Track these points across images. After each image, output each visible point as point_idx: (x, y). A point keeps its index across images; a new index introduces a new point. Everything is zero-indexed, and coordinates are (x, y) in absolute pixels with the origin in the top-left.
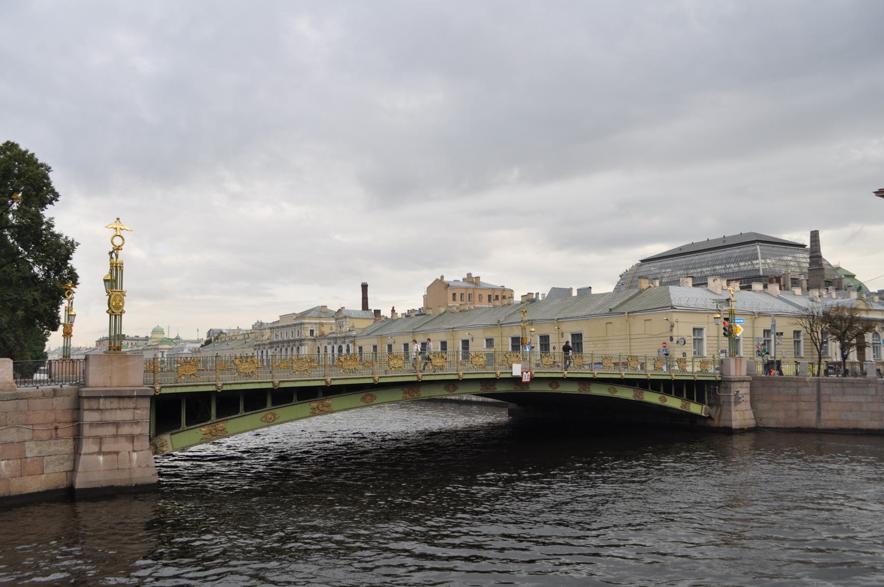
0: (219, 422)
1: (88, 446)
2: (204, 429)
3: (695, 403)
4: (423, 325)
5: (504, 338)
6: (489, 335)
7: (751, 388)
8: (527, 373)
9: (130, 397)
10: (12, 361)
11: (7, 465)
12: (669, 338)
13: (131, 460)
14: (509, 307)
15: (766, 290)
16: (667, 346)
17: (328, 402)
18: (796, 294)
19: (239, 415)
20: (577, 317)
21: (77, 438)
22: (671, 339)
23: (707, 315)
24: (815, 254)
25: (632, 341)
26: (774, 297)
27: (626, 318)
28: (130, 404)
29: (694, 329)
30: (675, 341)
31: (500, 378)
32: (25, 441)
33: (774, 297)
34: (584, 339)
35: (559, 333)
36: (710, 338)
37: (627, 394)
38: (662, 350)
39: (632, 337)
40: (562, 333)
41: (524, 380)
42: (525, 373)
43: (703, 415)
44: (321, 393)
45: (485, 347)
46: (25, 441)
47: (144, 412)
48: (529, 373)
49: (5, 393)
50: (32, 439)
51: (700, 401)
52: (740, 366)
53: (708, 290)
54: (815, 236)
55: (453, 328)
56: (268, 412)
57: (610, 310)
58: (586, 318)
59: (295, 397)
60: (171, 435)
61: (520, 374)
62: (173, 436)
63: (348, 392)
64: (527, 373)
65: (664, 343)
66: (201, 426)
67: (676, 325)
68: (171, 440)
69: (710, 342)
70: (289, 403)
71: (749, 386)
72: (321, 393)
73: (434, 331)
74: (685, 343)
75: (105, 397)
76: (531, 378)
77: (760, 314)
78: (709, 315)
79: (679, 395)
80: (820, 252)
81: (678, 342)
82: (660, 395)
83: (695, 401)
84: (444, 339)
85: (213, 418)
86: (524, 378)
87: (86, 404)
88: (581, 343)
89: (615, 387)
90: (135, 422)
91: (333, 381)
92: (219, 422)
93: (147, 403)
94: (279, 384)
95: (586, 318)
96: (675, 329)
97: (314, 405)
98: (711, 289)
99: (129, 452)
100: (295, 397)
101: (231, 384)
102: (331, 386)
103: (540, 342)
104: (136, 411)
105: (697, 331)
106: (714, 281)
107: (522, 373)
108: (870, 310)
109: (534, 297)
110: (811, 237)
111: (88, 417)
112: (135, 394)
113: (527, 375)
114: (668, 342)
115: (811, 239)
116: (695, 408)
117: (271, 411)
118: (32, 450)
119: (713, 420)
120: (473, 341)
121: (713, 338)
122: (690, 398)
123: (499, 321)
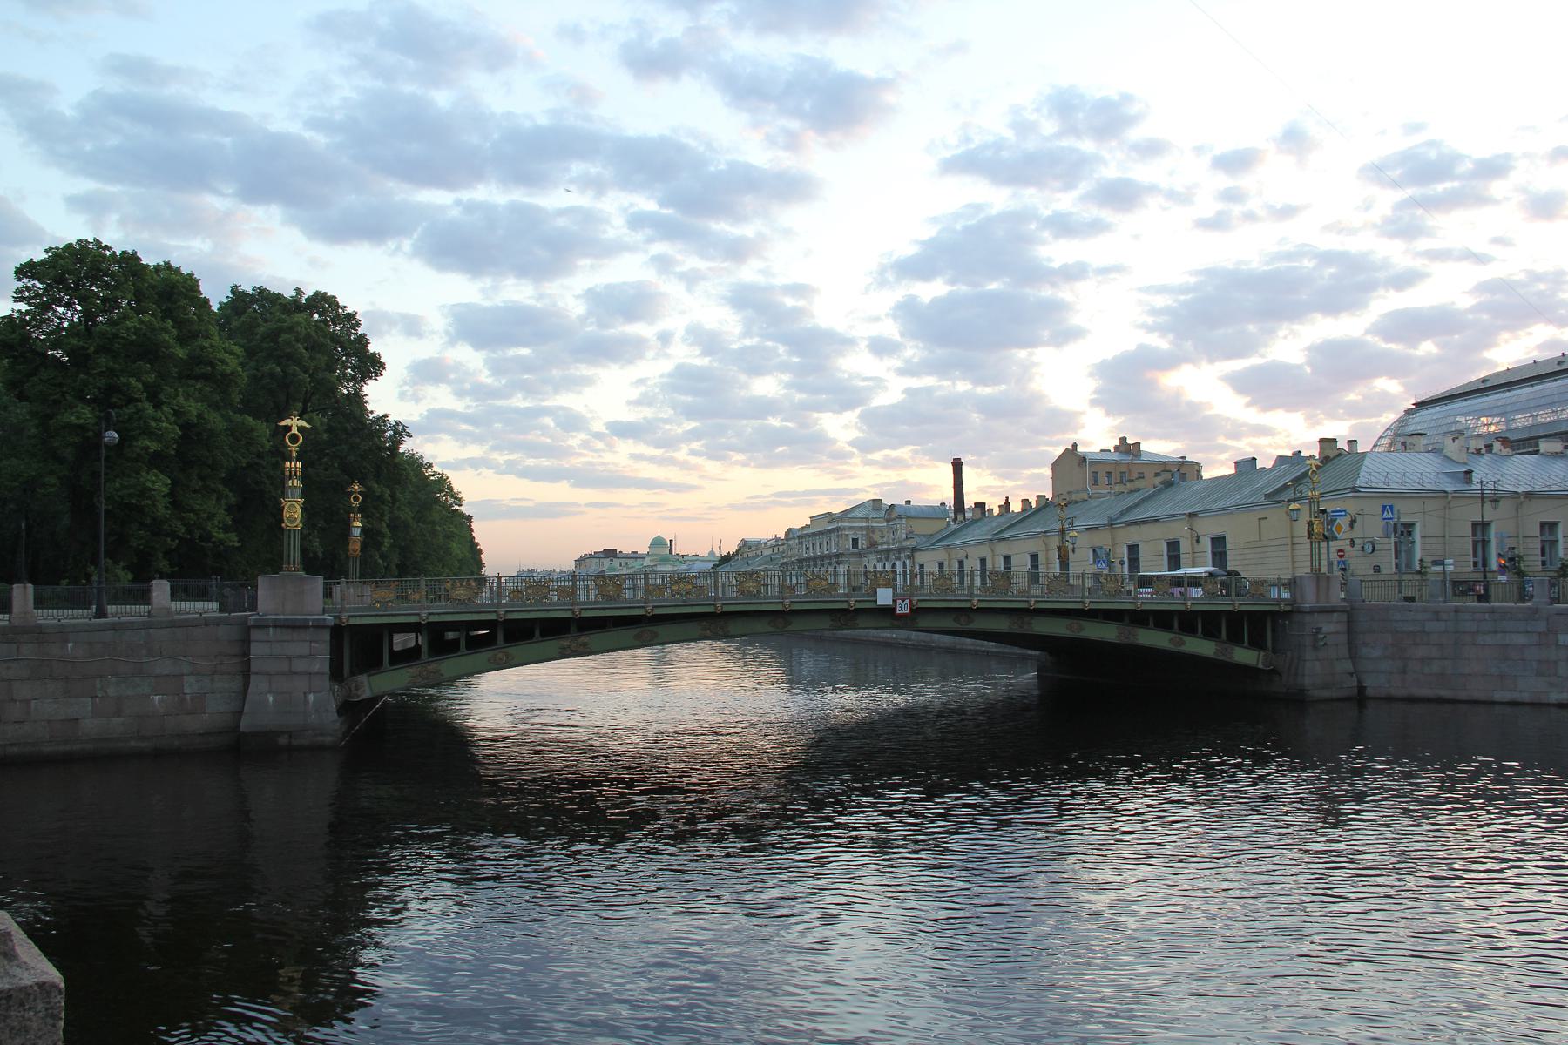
0: (432, 661)
1: (257, 684)
3: (1245, 648)
4: (1008, 528)
7: (1349, 622)
8: (903, 601)
10: (169, 583)
11: (161, 701)
12: (1348, 542)
13: (306, 701)
16: (1346, 555)
19: (459, 654)
20: (1218, 510)
21: (246, 675)
22: (1352, 543)
23: (1421, 501)
25: (1298, 547)
30: (1357, 547)
31: (978, 608)
32: (183, 675)
35: (1192, 538)
36: (1428, 540)
37: (1107, 633)
38: (1336, 563)
39: (1296, 541)
40: (1198, 537)
41: (898, 612)
42: (899, 602)
43: (1260, 666)
44: (573, 628)
46: (183, 675)
47: (322, 646)
48: (907, 601)
49: (159, 619)
50: (192, 674)
51: (1257, 643)
52: (1328, 588)
55: (1045, 532)
56: (497, 651)
58: (1229, 511)
59: (537, 633)
60: (369, 676)
61: (889, 602)
62: (371, 678)
63: (614, 626)
64: (903, 601)
65: (1341, 551)
66: (408, 666)
67: (1359, 519)
68: (369, 683)
69: (1428, 547)
70: (529, 639)
71: (1345, 619)
73: (1019, 538)
74: (1373, 550)
75: (275, 627)
76: (911, 609)
77: (1529, 495)
78: (1426, 501)
79: (1211, 633)
82: (1172, 635)
83: (1246, 644)
84: (1033, 550)
86: (898, 608)
87: (255, 635)
88: (1225, 553)
89: (1081, 622)
90: (312, 656)
91: (583, 612)
92: (432, 661)
94: (504, 615)
95: (1229, 511)
97: (565, 643)
98: (1449, 454)
99: (305, 693)
100: (537, 633)
101: (439, 614)
102: (580, 618)
104: (313, 645)
106: (1454, 440)
107: (894, 601)
111: (256, 649)
112: (311, 624)
113: (903, 604)
114: (1348, 549)
116: (1244, 656)
117: (503, 650)
118: (190, 686)
119: (1280, 675)
120: (1073, 551)
121: (1434, 540)
122: (1235, 638)
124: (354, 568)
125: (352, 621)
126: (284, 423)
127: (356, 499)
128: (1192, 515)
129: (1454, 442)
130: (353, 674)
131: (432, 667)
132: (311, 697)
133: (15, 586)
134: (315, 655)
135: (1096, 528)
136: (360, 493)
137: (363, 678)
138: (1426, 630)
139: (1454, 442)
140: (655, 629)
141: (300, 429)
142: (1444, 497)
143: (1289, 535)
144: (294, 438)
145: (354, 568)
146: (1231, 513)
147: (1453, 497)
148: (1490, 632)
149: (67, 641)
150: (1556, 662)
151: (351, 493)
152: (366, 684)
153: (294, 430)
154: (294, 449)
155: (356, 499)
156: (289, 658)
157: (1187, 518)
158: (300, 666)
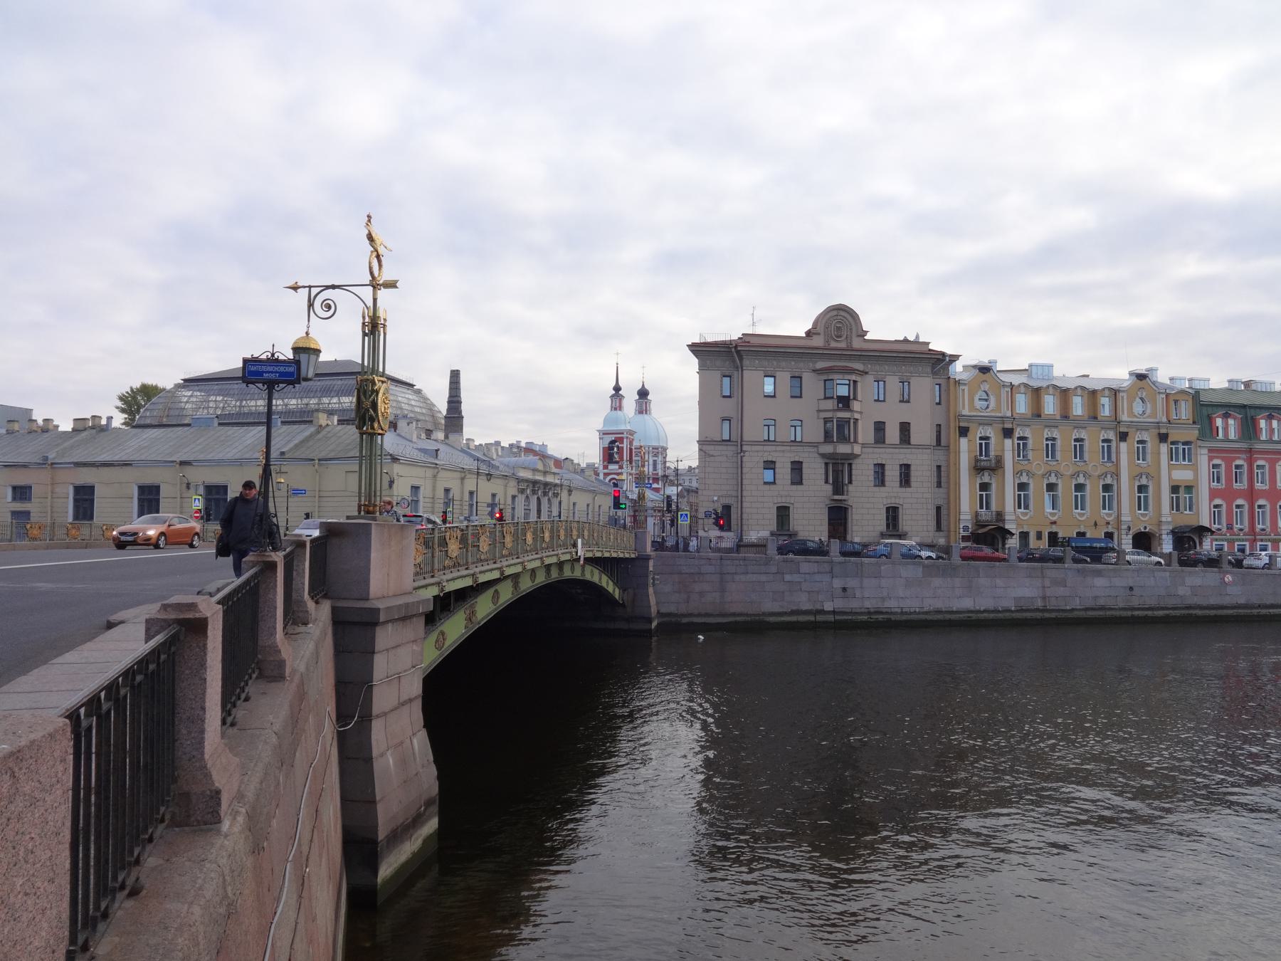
5: (58, 489)
6: (21, 479)
14: (46, 435)
15: (447, 441)
18: (471, 447)
23: (424, 469)
24: (455, 399)
26: (457, 449)
27: (316, 466)
29: (412, 487)
33: (457, 449)
34: (162, 494)
39: (322, 494)
45: (9, 498)
53: (399, 435)
54: (455, 376)
57: (283, 453)
78: (427, 469)
80: (460, 397)
81: (397, 503)
96: (395, 486)
98: (403, 434)
103: (139, 495)
105: (415, 489)
108: (548, 472)
109: (104, 422)
110: (451, 377)
115: (450, 379)
123: (46, 458)
128: (183, 463)
129: (408, 425)
135: (25, 466)
138: (702, 572)
139: (408, 425)
142: (434, 468)
143: (317, 490)
146: (241, 465)
147: (442, 469)
148: (743, 573)
150: (783, 592)
157: (178, 466)
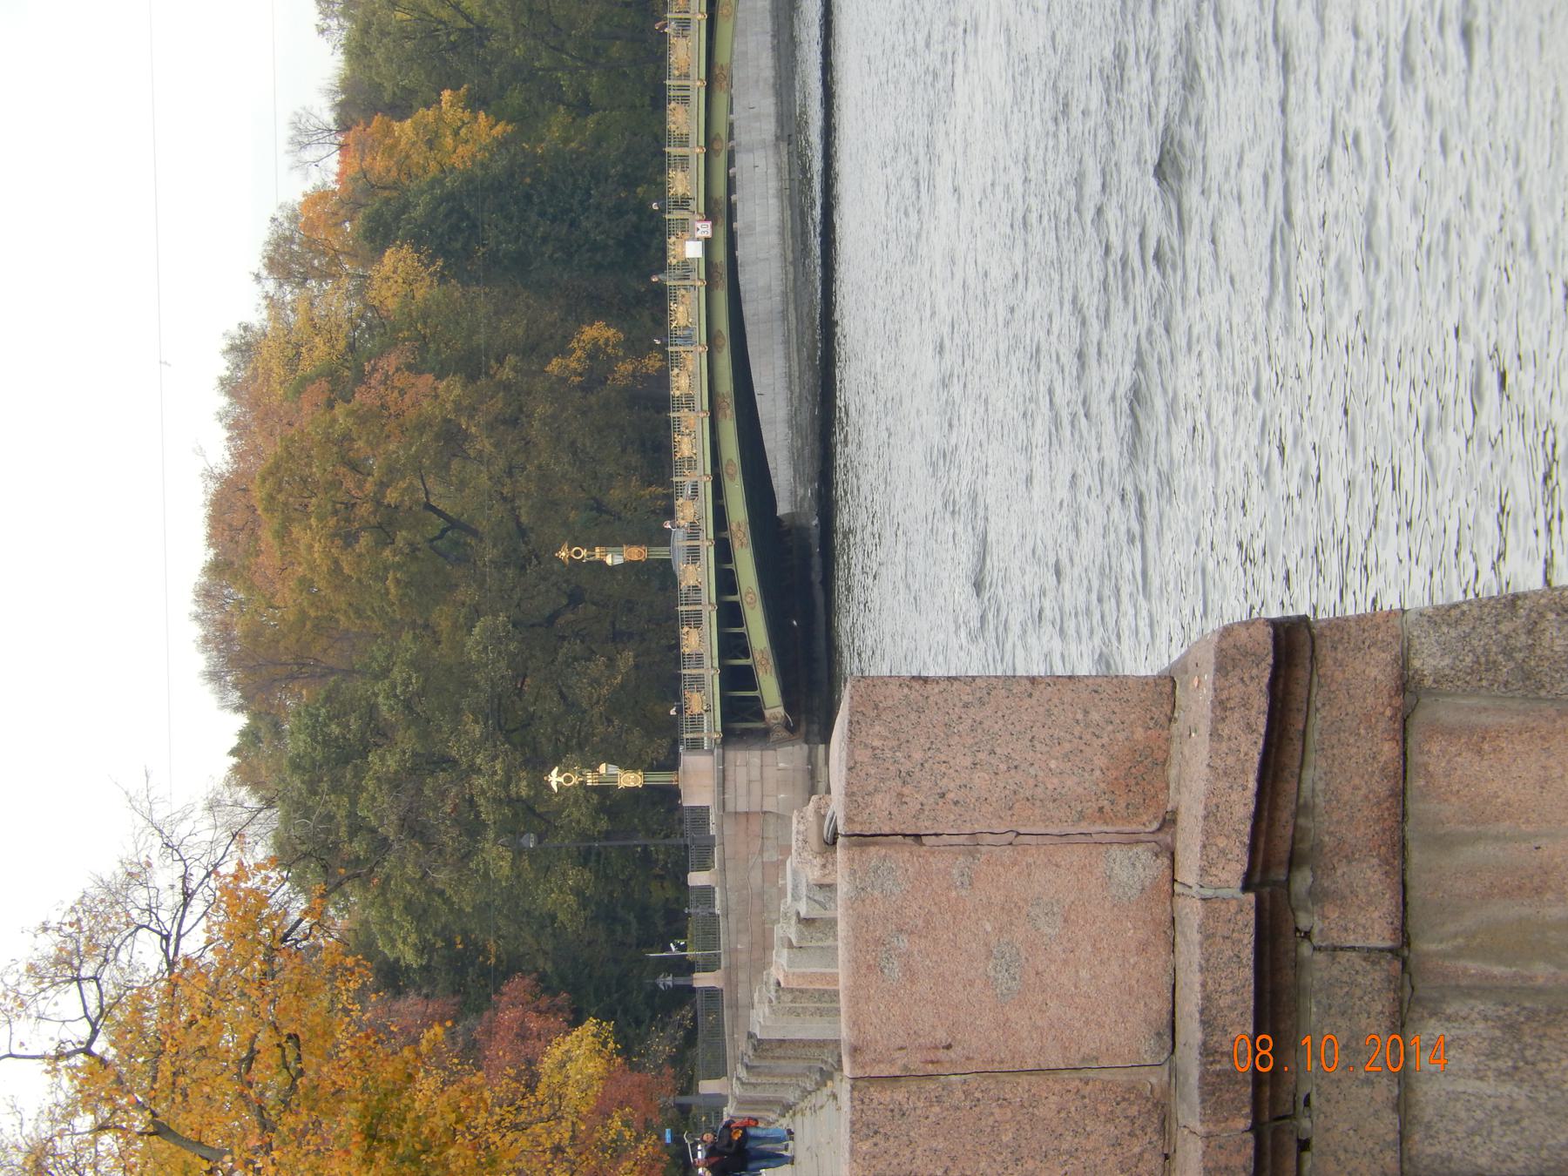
1: (770, 805)
2: (760, 674)
9: (724, 771)
17: (734, 527)
28: (730, 773)
42: (698, 234)
44: (723, 534)
59: (728, 566)
61: (700, 244)
72: (723, 534)
75: (724, 794)
85: (748, 662)
86: (705, 235)
90: (747, 764)
93: (730, 754)
97: (737, 544)
100: (728, 566)
107: (698, 239)
111: (742, 807)
124: (660, 553)
125: (719, 728)
126: (556, 789)
127: (578, 553)
130: (760, 716)
131: (758, 656)
132: (781, 765)
133: (690, 884)
134: (748, 762)
136: (570, 549)
137: (767, 713)
140: (724, 462)
141: (559, 774)
144: (568, 779)
145: (660, 553)
149: (736, 950)
151: (570, 558)
152: (771, 711)
153: (561, 780)
154: (575, 780)
155: (578, 553)
156: (750, 782)
158: (755, 774)
